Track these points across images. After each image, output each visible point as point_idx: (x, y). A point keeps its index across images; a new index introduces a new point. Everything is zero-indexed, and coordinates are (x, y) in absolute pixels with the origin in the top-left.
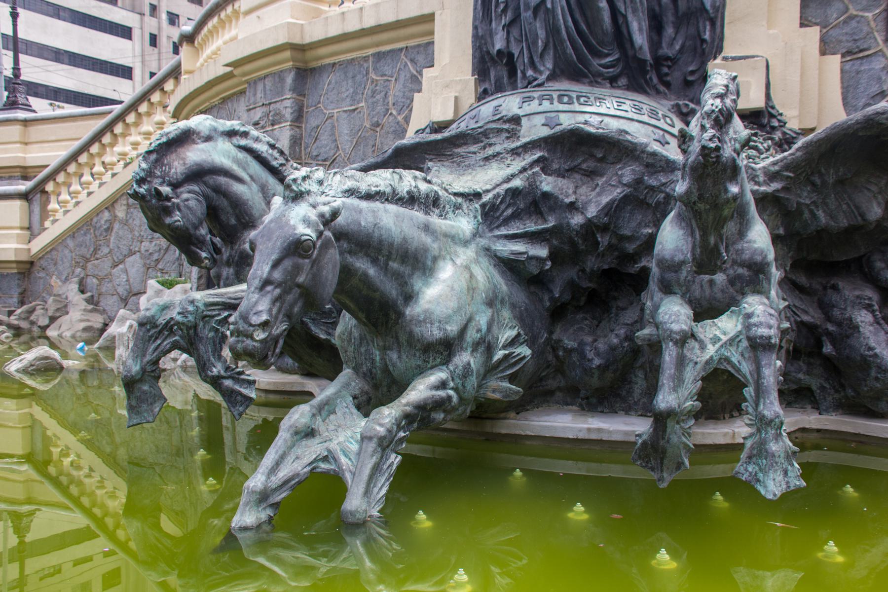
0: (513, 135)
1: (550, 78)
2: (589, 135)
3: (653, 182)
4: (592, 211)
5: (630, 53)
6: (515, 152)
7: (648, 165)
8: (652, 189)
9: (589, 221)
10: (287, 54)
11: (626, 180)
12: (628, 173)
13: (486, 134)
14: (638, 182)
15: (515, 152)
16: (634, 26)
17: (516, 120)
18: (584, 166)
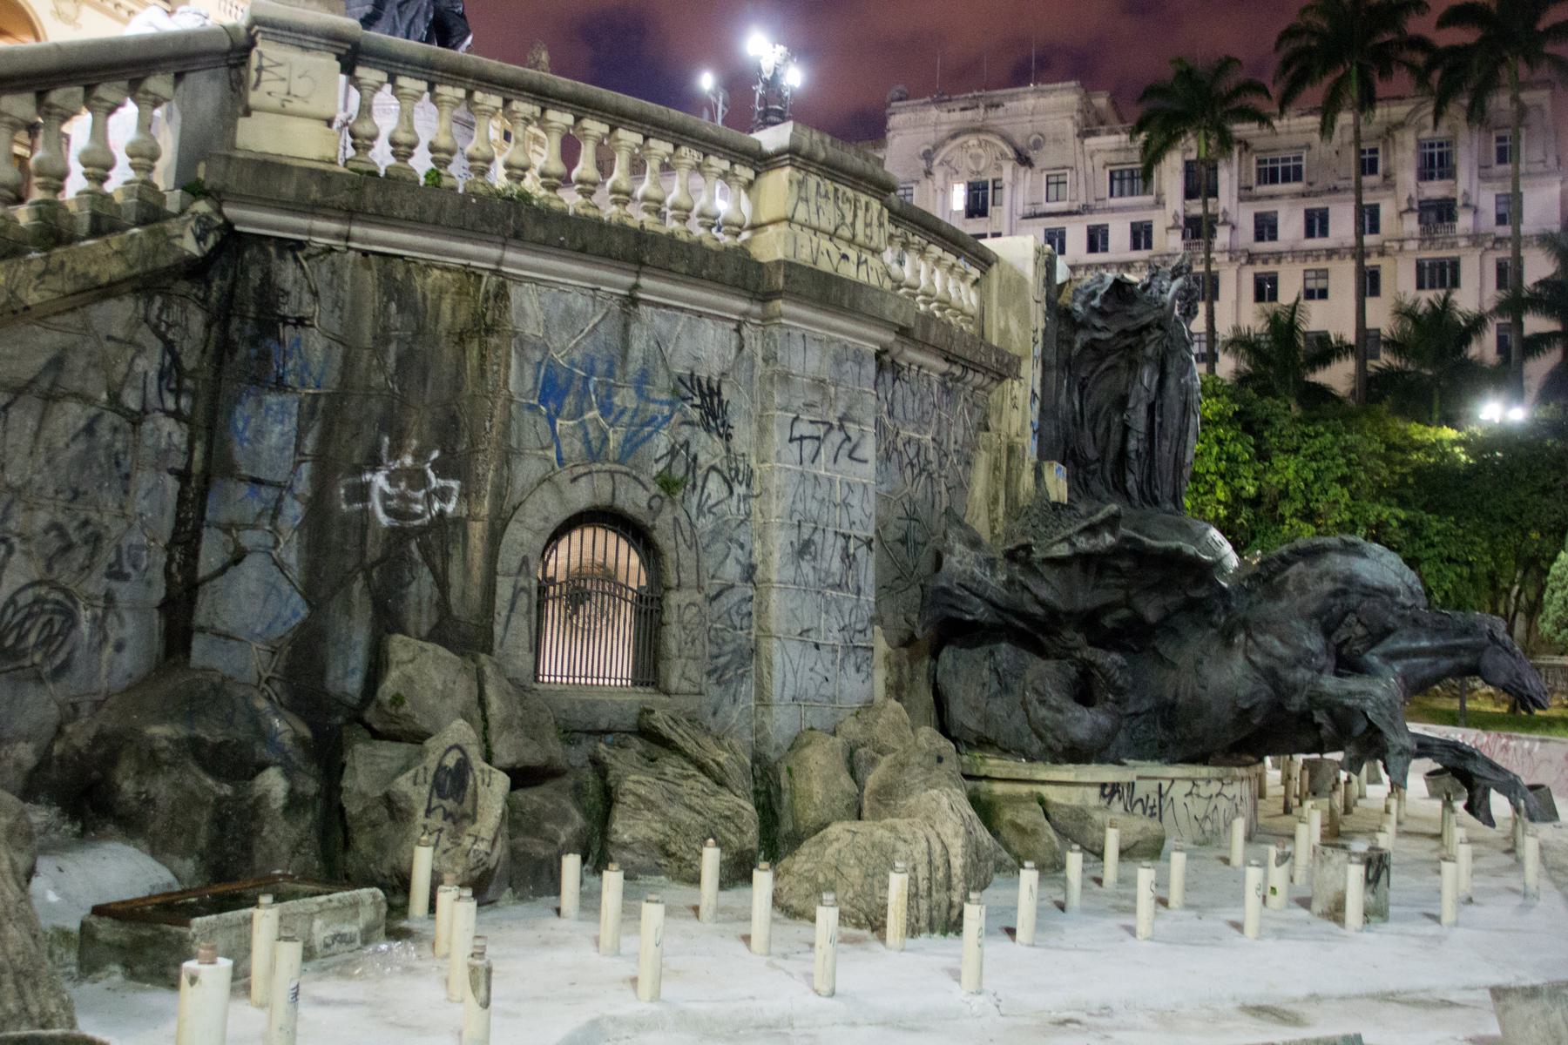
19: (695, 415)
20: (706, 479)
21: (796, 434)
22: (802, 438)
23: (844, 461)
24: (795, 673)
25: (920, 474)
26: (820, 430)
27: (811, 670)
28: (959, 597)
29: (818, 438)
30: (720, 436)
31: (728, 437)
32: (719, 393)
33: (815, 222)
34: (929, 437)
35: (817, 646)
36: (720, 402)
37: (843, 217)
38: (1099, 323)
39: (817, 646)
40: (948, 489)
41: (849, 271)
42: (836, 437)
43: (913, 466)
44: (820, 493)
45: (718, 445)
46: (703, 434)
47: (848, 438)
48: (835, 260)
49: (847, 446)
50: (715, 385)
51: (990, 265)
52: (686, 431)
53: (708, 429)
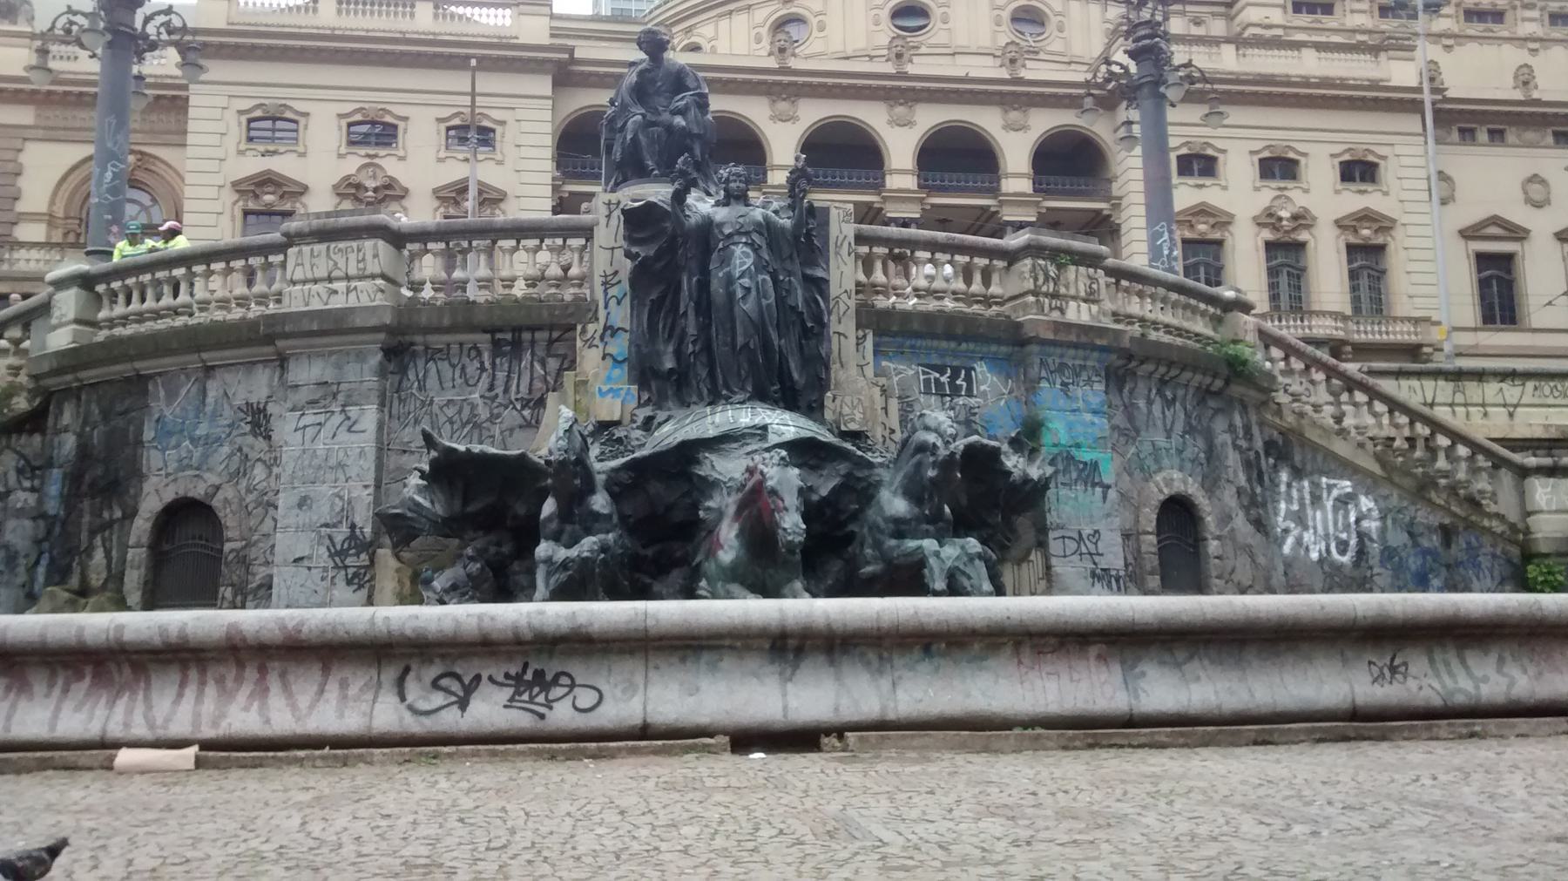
0: (763, 437)
1: (749, 399)
2: (820, 441)
3: (859, 474)
4: (824, 492)
5: (788, 384)
6: (768, 450)
7: (856, 464)
8: (859, 479)
9: (824, 499)
10: (382, 336)
11: (842, 472)
12: (843, 468)
13: (744, 436)
14: (848, 476)
15: (768, 450)
16: (792, 365)
17: (765, 428)
18: (811, 462)
19: (248, 428)
20: (253, 466)
21: (301, 424)
22: (305, 427)
23: (343, 436)
24: (288, 588)
25: (464, 425)
26: (321, 418)
27: (302, 586)
28: (409, 519)
29: (320, 424)
30: (264, 438)
31: (268, 438)
32: (265, 409)
33: (309, 276)
34: (477, 395)
35: (309, 568)
36: (265, 416)
37: (336, 264)
38: (634, 250)
39: (309, 568)
40: (502, 432)
41: (338, 303)
42: (337, 419)
43: (452, 423)
44: (316, 462)
45: (261, 443)
46: (250, 439)
47: (348, 418)
48: (325, 297)
49: (347, 423)
50: (261, 406)
51: (592, 230)
52: (239, 440)
53: (255, 436)
